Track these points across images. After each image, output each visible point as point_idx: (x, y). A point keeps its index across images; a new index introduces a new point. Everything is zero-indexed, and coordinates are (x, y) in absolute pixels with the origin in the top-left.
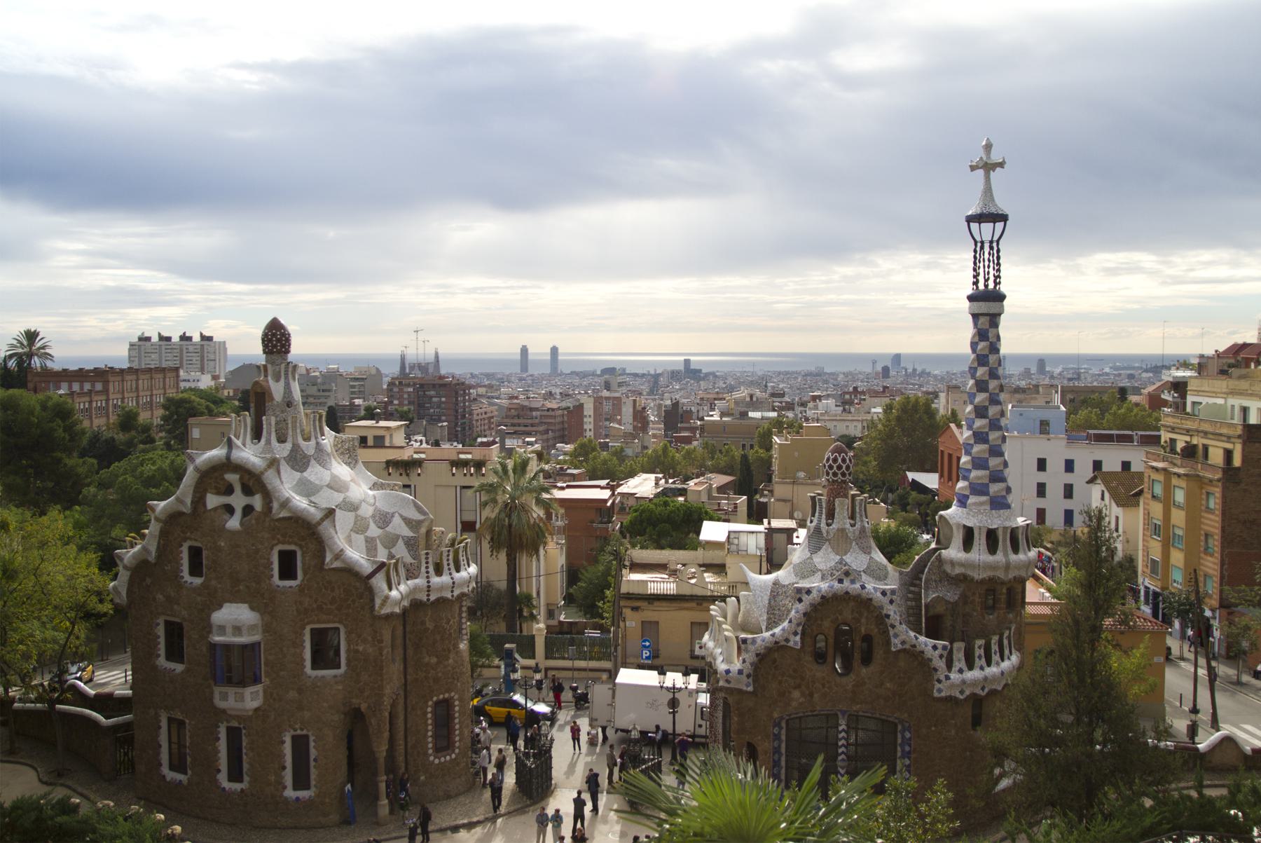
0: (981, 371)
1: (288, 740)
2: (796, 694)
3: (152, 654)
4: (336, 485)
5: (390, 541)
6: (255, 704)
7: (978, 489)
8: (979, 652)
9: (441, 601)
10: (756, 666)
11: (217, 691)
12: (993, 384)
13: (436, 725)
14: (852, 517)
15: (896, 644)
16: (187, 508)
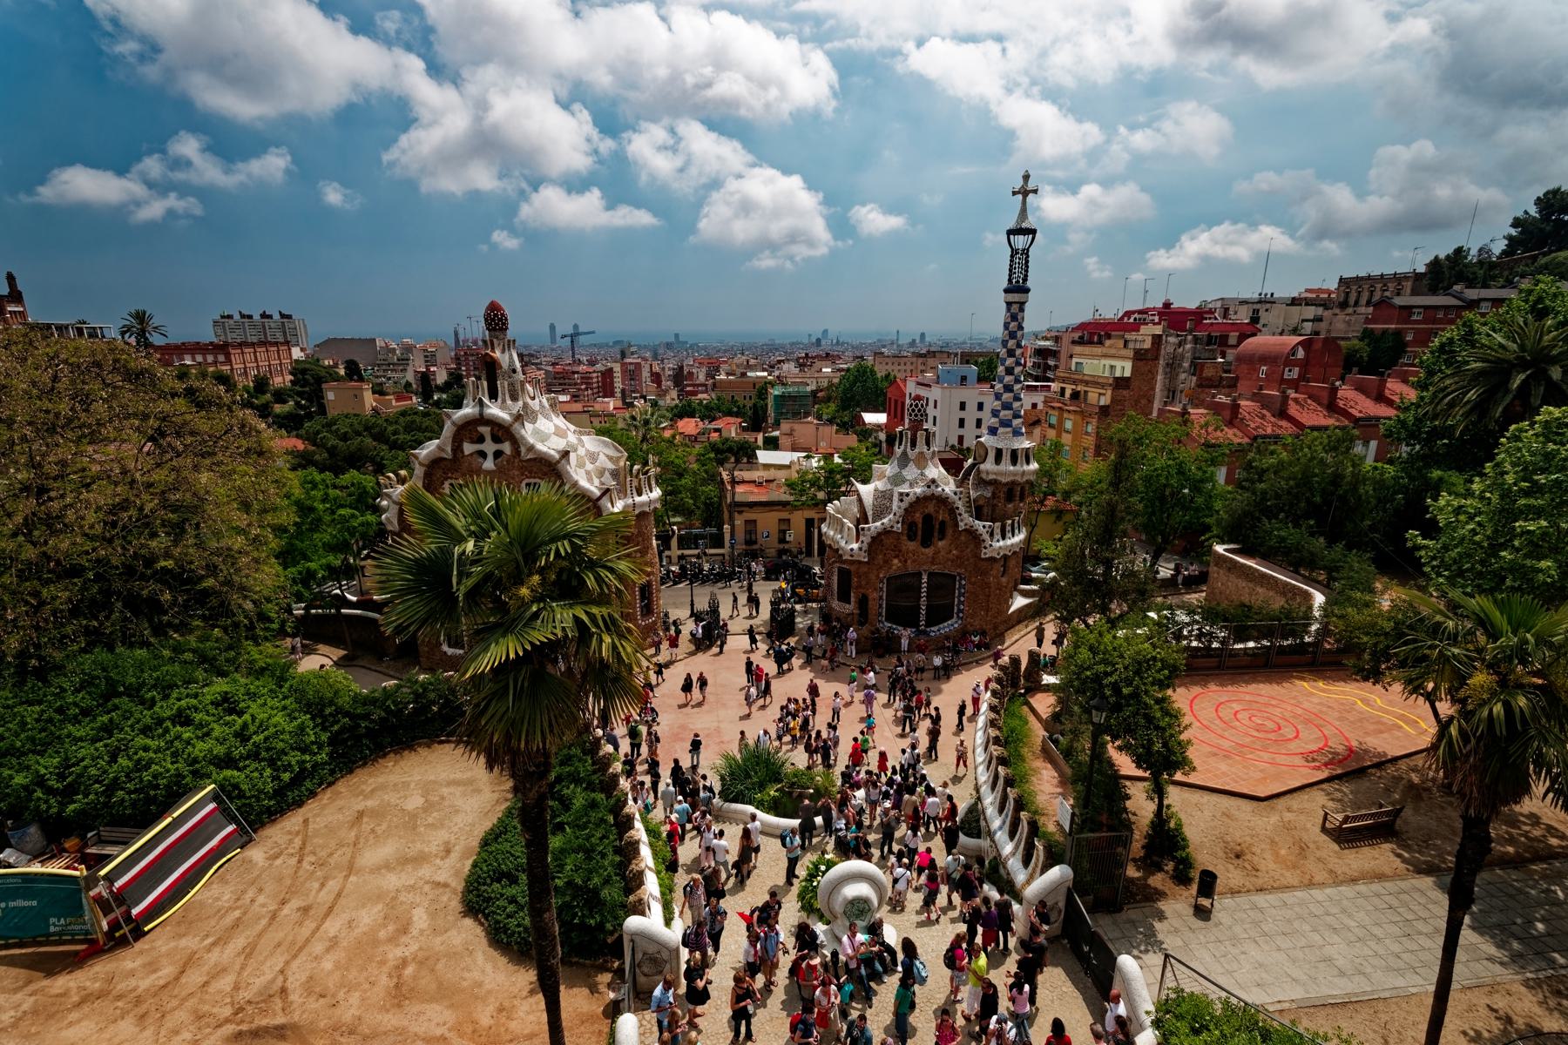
2: (896, 561)
5: (601, 473)
10: (870, 545)
14: (928, 444)
15: (962, 526)
16: (448, 453)
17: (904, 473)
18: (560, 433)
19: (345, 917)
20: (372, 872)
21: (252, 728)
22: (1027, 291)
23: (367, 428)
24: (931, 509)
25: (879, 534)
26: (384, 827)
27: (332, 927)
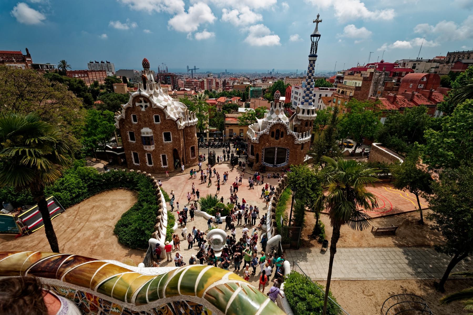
0: (310, 74)
1: (161, 156)
2: (267, 144)
3: (127, 139)
4: (166, 100)
5: (179, 113)
6: (154, 149)
7: (306, 101)
8: (304, 135)
9: (191, 126)
10: (259, 138)
11: (144, 146)
12: (312, 77)
13: (192, 152)
14: (280, 107)
16: (131, 106)
17: (272, 116)
18: (166, 100)
19: (83, 233)
20: (93, 222)
21: (65, 181)
22: (316, 56)
23: (118, 98)
24: (279, 128)
25: (262, 135)
26: (99, 210)
27: (79, 235)
